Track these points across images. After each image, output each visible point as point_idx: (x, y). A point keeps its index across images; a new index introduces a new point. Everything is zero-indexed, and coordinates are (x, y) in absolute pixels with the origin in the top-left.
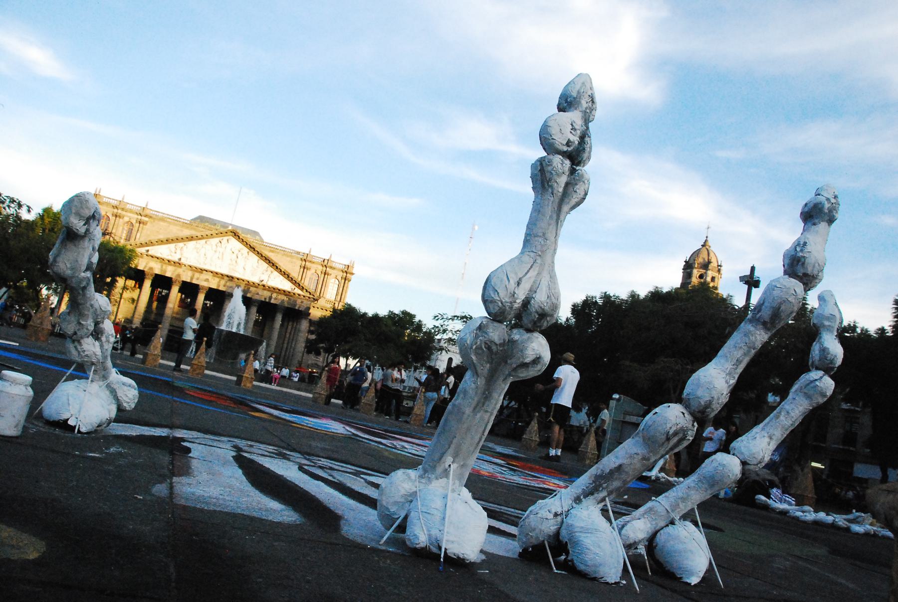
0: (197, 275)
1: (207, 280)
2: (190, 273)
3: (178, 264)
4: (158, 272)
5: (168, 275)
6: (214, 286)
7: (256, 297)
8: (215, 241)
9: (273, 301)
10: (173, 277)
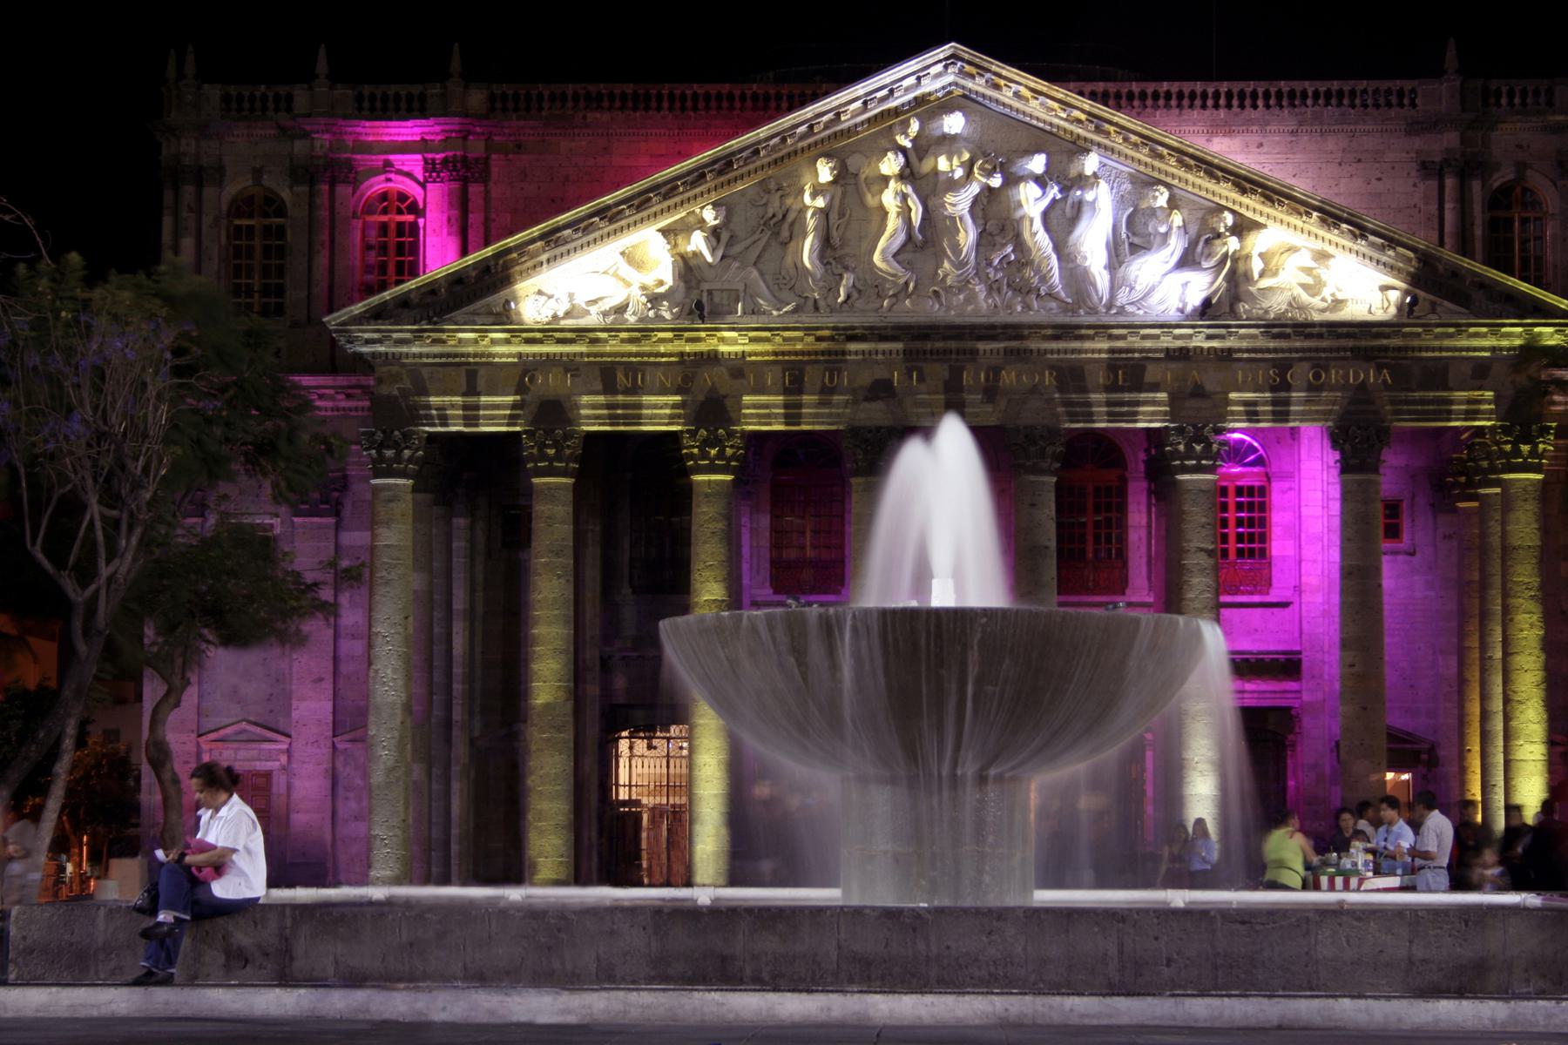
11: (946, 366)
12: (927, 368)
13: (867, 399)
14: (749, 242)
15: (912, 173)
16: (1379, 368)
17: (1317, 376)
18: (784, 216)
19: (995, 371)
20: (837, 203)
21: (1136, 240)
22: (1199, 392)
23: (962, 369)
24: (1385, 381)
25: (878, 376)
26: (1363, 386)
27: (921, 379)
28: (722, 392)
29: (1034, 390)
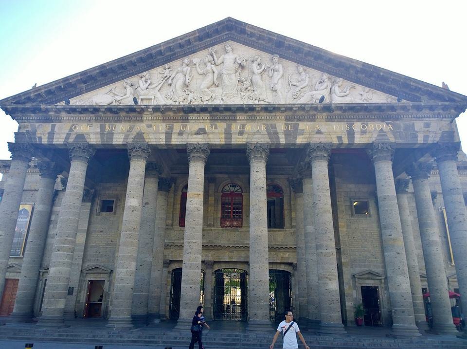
0: (177, 127)
1: (201, 132)
2: (162, 127)
4: (94, 139)
5: (118, 140)
7: (316, 139)
9: (359, 140)
10: (130, 140)
11: (225, 124)
12: (218, 124)
13: (197, 133)
14: (157, 84)
15: (215, 63)
16: (387, 124)
17: (364, 127)
18: (170, 77)
19: (243, 126)
20: (188, 72)
21: (292, 83)
22: (319, 132)
23: (231, 124)
24: (390, 129)
25: (200, 127)
27: (216, 128)
28: (143, 132)
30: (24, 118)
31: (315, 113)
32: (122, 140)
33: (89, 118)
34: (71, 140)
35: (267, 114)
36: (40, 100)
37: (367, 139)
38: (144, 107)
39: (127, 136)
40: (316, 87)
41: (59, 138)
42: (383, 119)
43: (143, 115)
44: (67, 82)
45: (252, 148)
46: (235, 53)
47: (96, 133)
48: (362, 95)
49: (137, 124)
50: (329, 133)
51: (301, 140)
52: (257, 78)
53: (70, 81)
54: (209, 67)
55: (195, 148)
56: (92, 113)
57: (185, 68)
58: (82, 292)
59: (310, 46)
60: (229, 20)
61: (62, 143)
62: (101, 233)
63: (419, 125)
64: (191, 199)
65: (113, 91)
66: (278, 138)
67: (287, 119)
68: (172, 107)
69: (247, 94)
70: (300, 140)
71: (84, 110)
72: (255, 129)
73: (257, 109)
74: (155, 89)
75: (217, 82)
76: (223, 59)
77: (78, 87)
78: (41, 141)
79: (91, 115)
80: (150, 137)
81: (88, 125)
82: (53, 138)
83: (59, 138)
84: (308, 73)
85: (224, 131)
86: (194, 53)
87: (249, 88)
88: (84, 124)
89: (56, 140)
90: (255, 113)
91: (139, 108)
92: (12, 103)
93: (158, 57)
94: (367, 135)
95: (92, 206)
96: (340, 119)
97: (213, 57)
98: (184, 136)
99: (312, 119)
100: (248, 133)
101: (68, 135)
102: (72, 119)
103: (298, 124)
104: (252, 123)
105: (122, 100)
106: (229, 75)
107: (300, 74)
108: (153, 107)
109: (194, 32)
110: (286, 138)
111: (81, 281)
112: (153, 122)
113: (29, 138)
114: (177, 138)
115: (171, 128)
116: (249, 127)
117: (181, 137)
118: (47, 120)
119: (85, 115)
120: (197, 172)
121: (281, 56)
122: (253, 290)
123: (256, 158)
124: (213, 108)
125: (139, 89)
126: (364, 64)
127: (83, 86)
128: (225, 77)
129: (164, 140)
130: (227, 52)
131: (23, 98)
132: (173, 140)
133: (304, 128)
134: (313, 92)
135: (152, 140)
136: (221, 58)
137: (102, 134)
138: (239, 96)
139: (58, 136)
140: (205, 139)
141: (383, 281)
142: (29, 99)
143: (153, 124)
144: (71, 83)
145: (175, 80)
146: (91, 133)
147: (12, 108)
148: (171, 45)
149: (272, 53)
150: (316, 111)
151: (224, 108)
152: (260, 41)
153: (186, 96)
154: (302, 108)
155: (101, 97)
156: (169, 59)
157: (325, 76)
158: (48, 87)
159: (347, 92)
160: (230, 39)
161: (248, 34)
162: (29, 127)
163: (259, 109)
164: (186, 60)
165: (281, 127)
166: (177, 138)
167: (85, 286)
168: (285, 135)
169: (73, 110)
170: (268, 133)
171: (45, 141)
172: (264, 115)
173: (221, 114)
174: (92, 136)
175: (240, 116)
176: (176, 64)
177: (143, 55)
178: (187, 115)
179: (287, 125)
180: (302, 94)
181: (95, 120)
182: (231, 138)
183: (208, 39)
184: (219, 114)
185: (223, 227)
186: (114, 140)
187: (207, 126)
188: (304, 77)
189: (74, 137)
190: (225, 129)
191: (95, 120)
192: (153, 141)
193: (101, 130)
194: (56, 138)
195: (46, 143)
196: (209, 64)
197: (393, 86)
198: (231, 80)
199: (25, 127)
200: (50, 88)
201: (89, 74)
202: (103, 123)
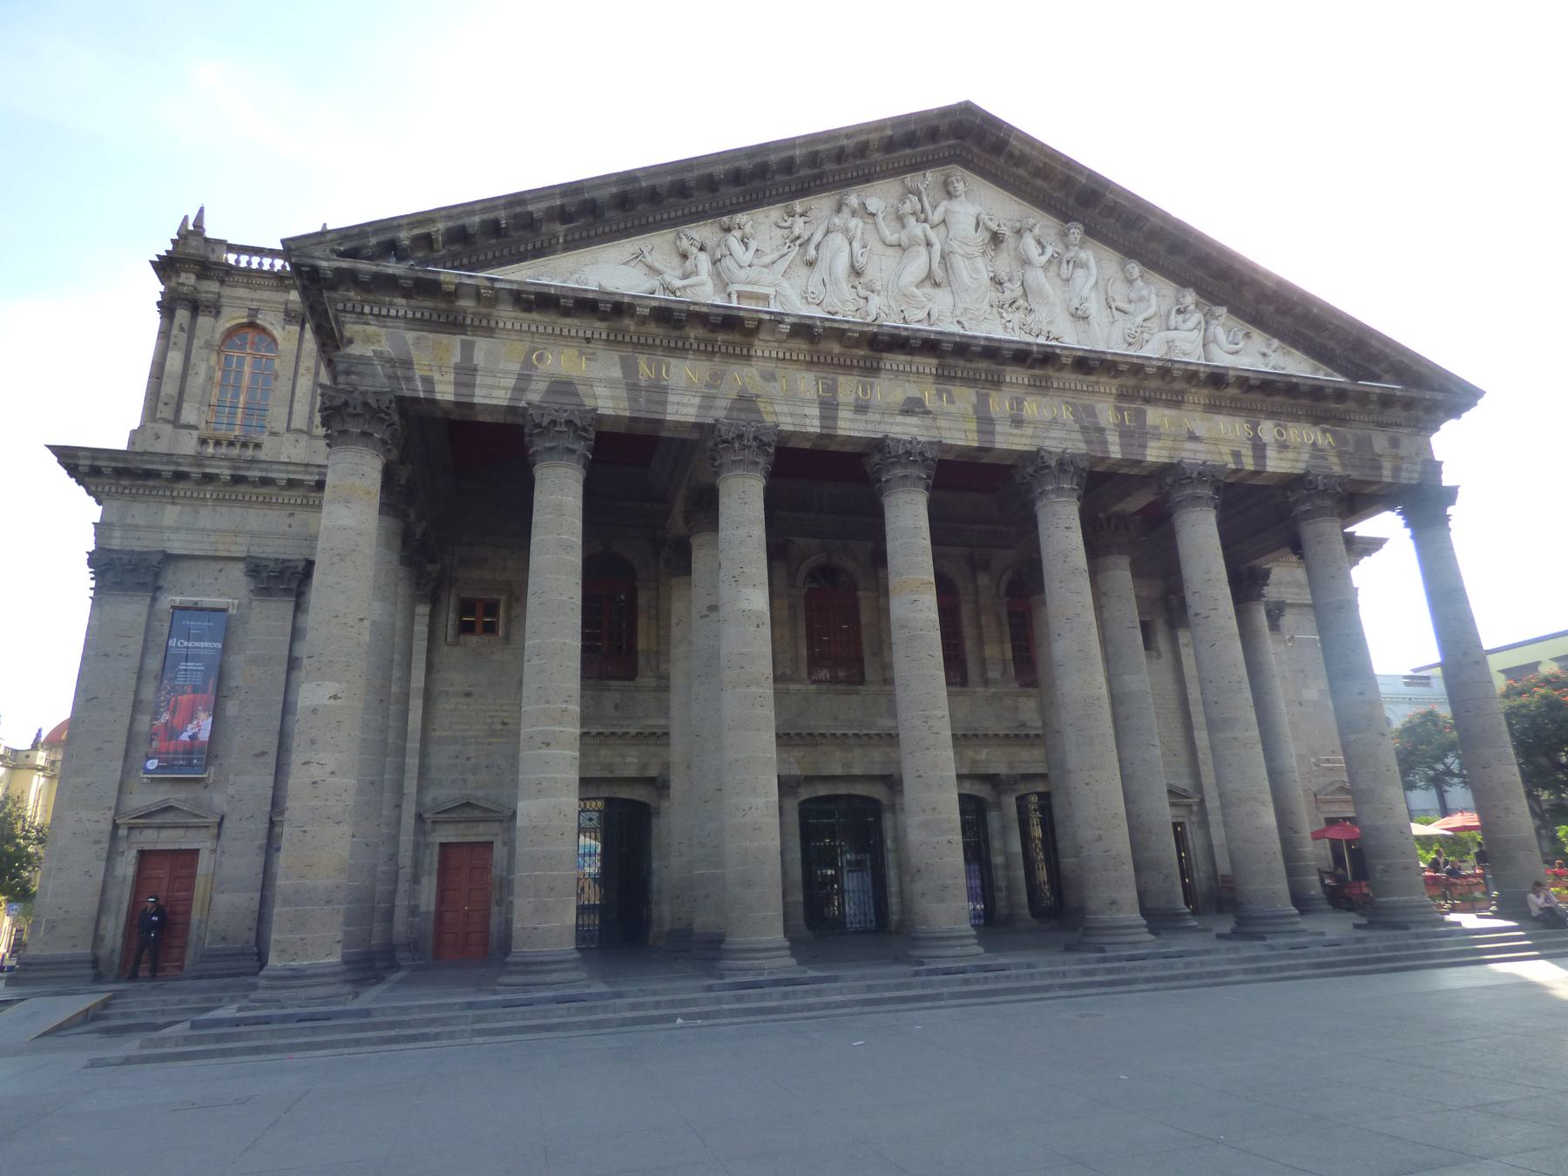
0: (848, 387)
1: (912, 407)
2: (807, 383)
3: (729, 330)
5: (682, 408)
6: (961, 434)
7: (1194, 455)
8: (879, 197)
9: (1276, 463)
10: (719, 412)
13: (906, 412)
14: (776, 255)
16: (1324, 431)
17: (1280, 434)
19: (1018, 403)
20: (859, 232)
22: (1193, 437)
23: (988, 395)
26: (1314, 444)
27: (951, 401)
28: (753, 391)
29: (1054, 421)
30: (367, 309)
31: (1185, 386)
32: (693, 411)
33: (589, 335)
34: (535, 397)
35: (1081, 377)
36: (420, 254)
37: (1289, 464)
38: (767, 317)
39: (708, 400)
40: (1172, 323)
41: (492, 387)
42: (1317, 419)
43: (756, 342)
44: (519, 209)
45: (1053, 463)
46: (975, 205)
47: (610, 383)
48: (1264, 355)
49: (733, 367)
50: (1216, 441)
51: (1155, 452)
52: (1036, 277)
53: (530, 208)
54: (916, 228)
55: (908, 453)
56: (604, 317)
57: (855, 224)
58: (424, 880)
59: (1165, 217)
60: (967, 109)
61: (505, 403)
62: (468, 700)
63: (1380, 441)
64: (916, 597)
65: (649, 259)
66: (1105, 443)
67: (1122, 396)
68: (846, 326)
69: (1016, 317)
70: (1155, 454)
71: (586, 306)
72: (1047, 415)
73: (1064, 360)
74: (762, 265)
75: (939, 274)
76: (946, 211)
77: (544, 229)
78: (433, 392)
79: (598, 324)
80: (778, 408)
81: (581, 354)
82: (474, 386)
83: (492, 387)
84: (1147, 283)
85: (971, 410)
86: (868, 181)
87: (1021, 302)
88: (567, 351)
89: (485, 392)
90: (1050, 372)
91: (752, 319)
92: (333, 251)
93: (779, 178)
94: (1290, 455)
95: (433, 615)
96: (1235, 409)
97: (920, 200)
98: (870, 416)
99: (1176, 402)
100: (1034, 423)
101: (524, 379)
102: (533, 328)
103: (1144, 412)
104: (1039, 398)
105: (685, 287)
106: (968, 257)
107: (1130, 282)
108: (794, 320)
109: (881, 125)
110: (1122, 445)
111: (417, 846)
112: (780, 365)
113: (390, 377)
114: (852, 420)
115: (832, 389)
116: (1033, 407)
117: (864, 417)
118: (453, 324)
119: (576, 321)
120: (908, 518)
121: (1091, 232)
122: (1099, 839)
123: (1059, 491)
124: (955, 343)
125: (728, 262)
126: (1281, 283)
127: (560, 229)
128: (960, 263)
129: (817, 423)
130: (950, 195)
131: (373, 241)
132: (841, 424)
133: (1157, 422)
134: (1172, 334)
135: (782, 419)
136: (941, 208)
137: (633, 387)
138: (998, 320)
139: (489, 381)
140: (927, 428)
141: (1195, 808)
142: (391, 248)
143: (779, 373)
144: (531, 213)
145: (825, 252)
146: (602, 382)
147: (338, 270)
148: (821, 147)
149: (1065, 217)
150: (1189, 382)
151: (985, 348)
152: (1038, 182)
153: (862, 302)
154: (1165, 371)
155: (609, 270)
156: (806, 189)
157: (1190, 297)
158: (459, 216)
159: (1242, 344)
160: (955, 162)
161: (1011, 155)
162: (384, 339)
163: (1069, 361)
164: (853, 200)
165: (1107, 414)
166: (852, 420)
167: (432, 859)
168: (1121, 436)
169: (544, 301)
170: (1082, 427)
171: (445, 392)
172: (1073, 379)
173: (969, 365)
174: (600, 390)
175: (1015, 375)
176: (821, 204)
177: (745, 164)
178: (877, 355)
179: (1120, 410)
180: (1146, 336)
181: (608, 341)
182: (992, 433)
183: (908, 151)
184: (962, 363)
185: (815, 682)
186: (670, 409)
187: (928, 394)
188: (1145, 292)
189: (542, 386)
190: (975, 408)
191: (608, 341)
192: (787, 424)
193: (625, 375)
194: (483, 386)
195: (451, 398)
196: (912, 220)
197: (1331, 344)
198: (973, 270)
199: (368, 339)
200: (466, 221)
201: (586, 196)
202: (627, 352)
